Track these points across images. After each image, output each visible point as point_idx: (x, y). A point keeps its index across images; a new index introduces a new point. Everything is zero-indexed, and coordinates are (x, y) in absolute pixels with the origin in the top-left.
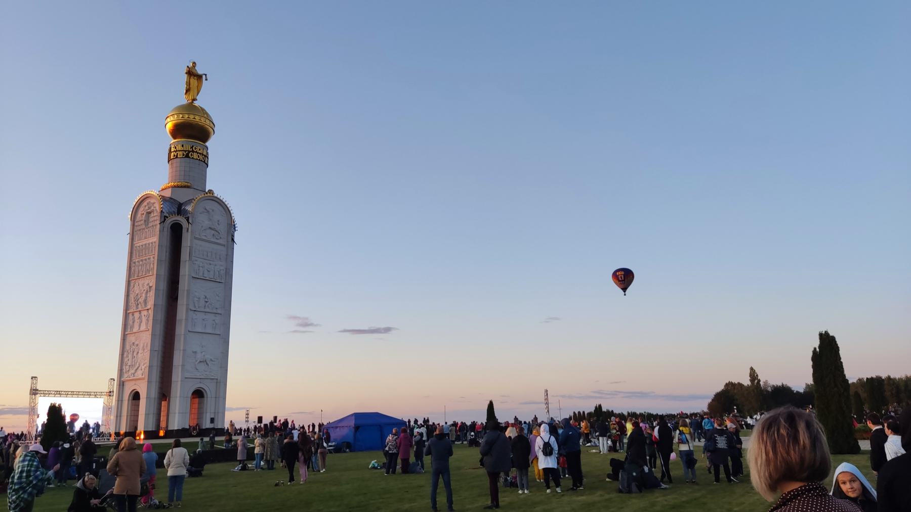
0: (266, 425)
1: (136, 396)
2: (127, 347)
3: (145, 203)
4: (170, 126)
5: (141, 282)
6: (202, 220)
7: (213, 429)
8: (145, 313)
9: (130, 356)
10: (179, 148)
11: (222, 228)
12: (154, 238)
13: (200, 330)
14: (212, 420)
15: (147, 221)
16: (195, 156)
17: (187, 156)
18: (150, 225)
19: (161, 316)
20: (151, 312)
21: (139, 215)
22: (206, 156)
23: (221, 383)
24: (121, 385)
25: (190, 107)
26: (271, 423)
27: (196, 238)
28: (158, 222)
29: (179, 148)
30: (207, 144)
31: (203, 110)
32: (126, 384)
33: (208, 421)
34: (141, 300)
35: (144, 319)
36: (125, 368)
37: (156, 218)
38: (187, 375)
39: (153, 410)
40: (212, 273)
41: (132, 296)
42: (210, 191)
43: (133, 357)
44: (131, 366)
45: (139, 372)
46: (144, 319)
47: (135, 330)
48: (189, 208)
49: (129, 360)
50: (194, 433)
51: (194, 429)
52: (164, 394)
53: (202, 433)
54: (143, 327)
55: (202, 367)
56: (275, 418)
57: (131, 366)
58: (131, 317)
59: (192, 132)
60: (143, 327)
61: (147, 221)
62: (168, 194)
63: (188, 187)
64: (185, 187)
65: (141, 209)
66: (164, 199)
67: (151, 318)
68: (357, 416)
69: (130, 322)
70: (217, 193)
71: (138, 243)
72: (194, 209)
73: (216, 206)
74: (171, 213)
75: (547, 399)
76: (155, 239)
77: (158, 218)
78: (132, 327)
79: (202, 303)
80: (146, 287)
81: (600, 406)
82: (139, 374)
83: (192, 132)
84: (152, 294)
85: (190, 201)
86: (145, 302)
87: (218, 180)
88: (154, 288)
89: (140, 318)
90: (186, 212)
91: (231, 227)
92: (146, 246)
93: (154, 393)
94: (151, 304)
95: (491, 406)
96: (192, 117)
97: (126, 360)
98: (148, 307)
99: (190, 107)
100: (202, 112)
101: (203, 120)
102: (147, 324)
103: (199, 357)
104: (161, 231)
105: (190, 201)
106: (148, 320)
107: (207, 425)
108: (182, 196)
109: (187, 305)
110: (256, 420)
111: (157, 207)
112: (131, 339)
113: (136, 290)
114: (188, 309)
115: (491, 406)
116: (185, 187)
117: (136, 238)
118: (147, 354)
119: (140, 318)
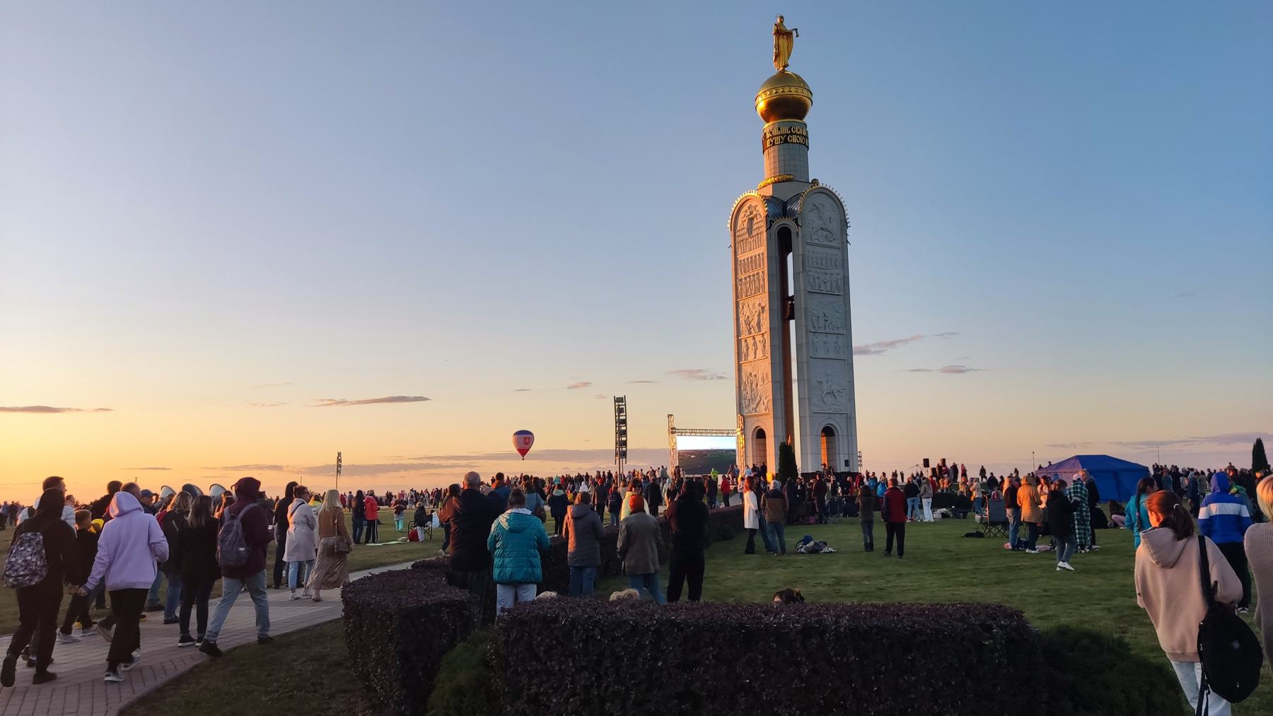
0: (934, 470)
1: (761, 434)
2: (744, 378)
3: (745, 208)
4: (762, 105)
5: (750, 301)
6: (812, 220)
9: (748, 389)
10: (776, 132)
11: (834, 226)
12: (759, 249)
14: (847, 463)
15: (750, 230)
16: (794, 139)
17: (786, 141)
18: (754, 233)
20: (767, 337)
21: (740, 223)
22: (806, 137)
23: (850, 418)
25: (783, 78)
26: (940, 467)
27: (808, 244)
28: (764, 229)
29: (776, 132)
30: (805, 120)
31: (798, 77)
34: (754, 323)
35: (760, 346)
37: (760, 224)
38: (815, 409)
40: (828, 285)
41: (742, 320)
42: (815, 182)
43: (752, 390)
44: (752, 400)
46: (760, 346)
47: (751, 358)
48: (796, 207)
55: (829, 399)
56: (944, 461)
57: (749, 397)
58: (743, 344)
59: (788, 108)
61: (750, 230)
62: (769, 192)
63: (790, 180)
64: (787, 180)
65: (742, 214)
66: (768, 201)
67: (768, 344)
68: (1084, 460)
70: (823, 182)
71: (741, 257)
72: (802, 206)
73: (821, 200)
74: (776, 216)
76: (763, 249)
77: (763, 224)
79: (822, 322)
80: (758, 308)
82: (762, 408)
83: (788, 108)
84: (766, 315)
85: (797, 197)
86: (759, 324)
87: (821, 168)
88: (767, 308)
89: (755, 344)
90: (792, 213)
91: (844, 224)
92: (752, 261)
94: (766, 326)
96: (787, 90)
99: (783, 78)
100: (798, 81)
101: (800, 90)
102: (764, 351)
104: (769, 239)
105: (797, 197)
107: (842, 468)
108: (786, 193)
109: (806, 326)
111: (762, 210)
112: (746, 369)
113: (746, 312)
114: (808, 332)
116: (787, 180)
117: (739, 251)
118: (769, 386)
119: (755, 344)
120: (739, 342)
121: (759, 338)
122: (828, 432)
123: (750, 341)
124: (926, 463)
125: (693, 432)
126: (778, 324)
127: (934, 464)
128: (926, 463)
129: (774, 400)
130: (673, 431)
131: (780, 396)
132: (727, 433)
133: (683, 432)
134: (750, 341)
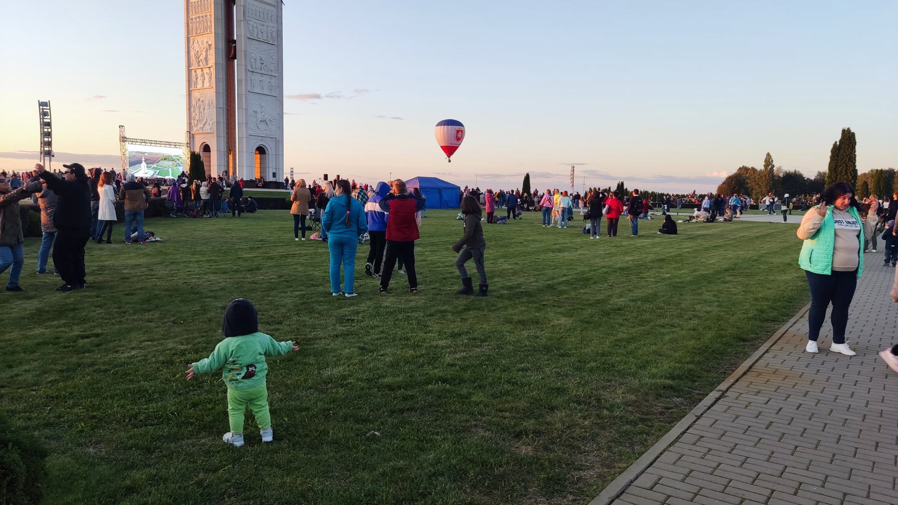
1: (207, 148)
2: (194, 103)
7: (276, 182)
8: (206, 71)
9: (197, 111)
13: (267, 93)
14: (274, 175)
19: (222, 75)
20: (213, 70)
24: (191, 136)
32: (196, 136)
33: (271, 175)
34: (202, 58)
35: (207, 77)
36: (194, 122)
38: (251, 133)
39: (224, 162)
41: (192, 53)
45: (207, 127)
46: (207, 77)
47: (199, 86)
49: (196, 114)
50: (260, 185)
51: (260, 181)
52: (230, 148)
53: (267, 185)
54: (207, 84)
55: (262, 126)
57: (197, 118)
60: (207, 84)
67: (214, 76)
68: (421, 179)
69: (194, 79)
75: (573, 175)
78: (196, 83)
79: (259, 65)
81: (622, 184)
84: (212, 52)
89: (203, 75)
93: (223, 147)
94: (212, 61)
95: (527, 179)
97: (193, 114)
98: (210, 65)
102: (210, 81)
103: (260, 116)
106: (210, 78)
107: (270, 178)
109: (246, 66)
110: (323, 177)
112: (196, 95)
114: (246, 70)
115: (527, 179)
119: (203, 75)
120: (189, 72)
121: (206, 71)
122: (261, 150)
123: (199, 72)
124: (326, 177)
125: (144, 142)
126: (222, 60)
127: (332, 178)
128: (326, 177)
129: (218, 123)
130: (123, 139)
131: (223, 119)
132: (176, 145)
133: (133, 141)
134: (199, 72)
